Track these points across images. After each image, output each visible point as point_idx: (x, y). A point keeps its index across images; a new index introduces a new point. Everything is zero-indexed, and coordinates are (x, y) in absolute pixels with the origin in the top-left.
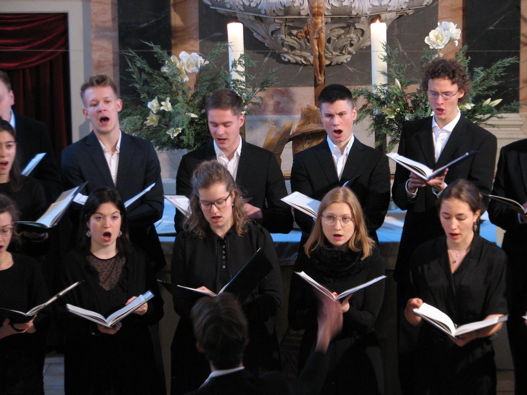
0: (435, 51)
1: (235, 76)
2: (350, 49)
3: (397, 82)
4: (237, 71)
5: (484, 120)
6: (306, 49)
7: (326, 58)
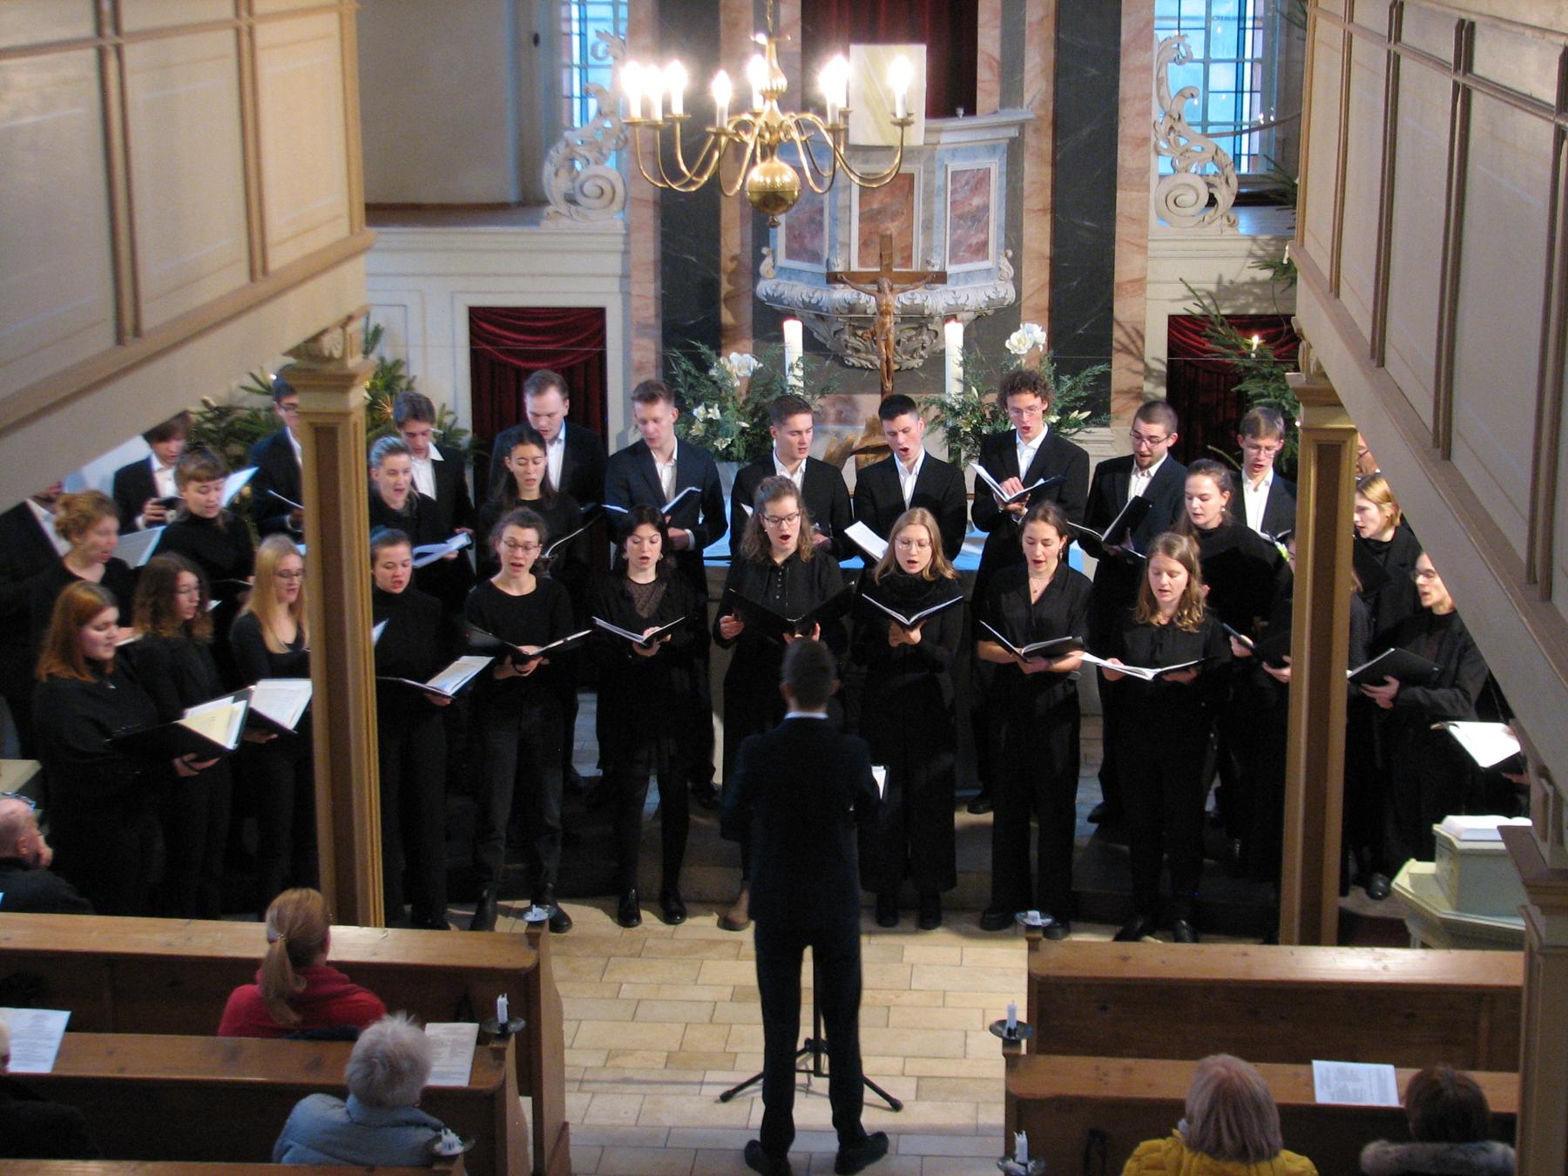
0: (1017, 357)
1: (792, 381)
2: (922, 353)
3: (974, 390)
4: (794, 376)
5: (1071, 435)
6: (873, 352)
7: (895, 362)
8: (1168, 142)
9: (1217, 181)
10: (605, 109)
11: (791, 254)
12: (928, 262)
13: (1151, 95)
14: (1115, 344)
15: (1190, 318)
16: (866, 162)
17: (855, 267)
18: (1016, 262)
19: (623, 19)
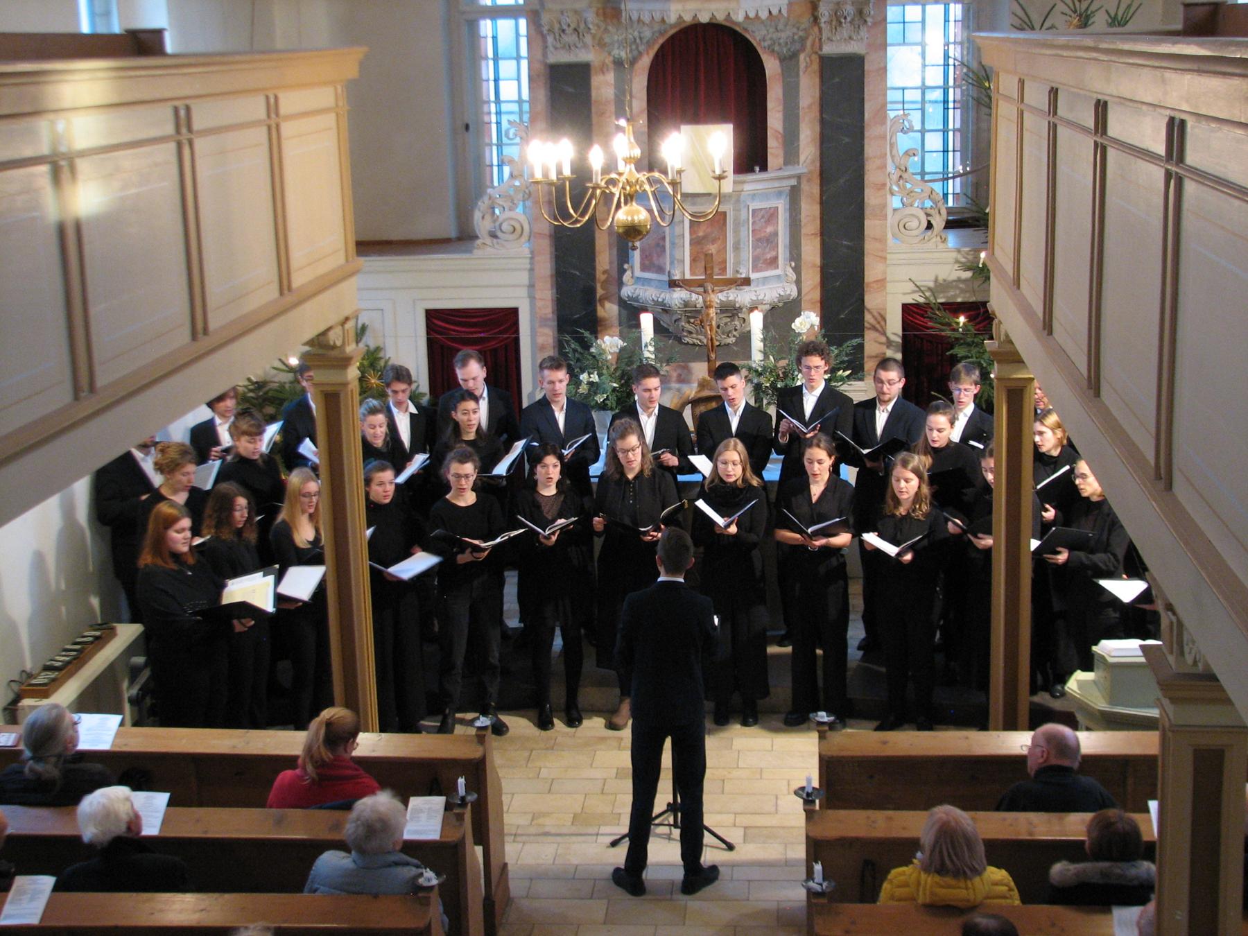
0: (800, 334)
1: (647, 354)
2: (735, 333)
3: (771, 358)
7: (717, 340)
8: (899, 186)
9: (932, 212)
10: (515, 173)
11: (644, 268)
12: (737, 272)
13: (886, 154)
14: (866, 324)
15: (917, 305)
16: (694, 204)
17: (688, 276)
18: (797, 270)
19: (527, 112)
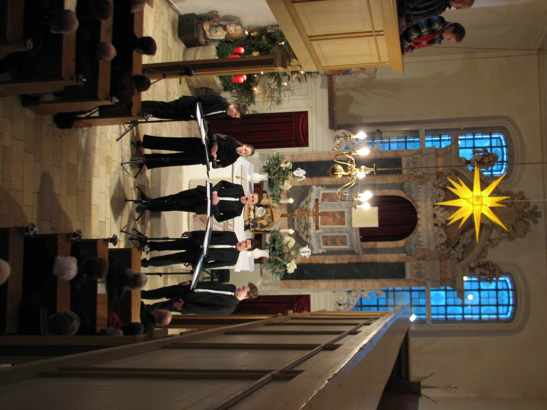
11: (324, 194)
18: (323, 254)
